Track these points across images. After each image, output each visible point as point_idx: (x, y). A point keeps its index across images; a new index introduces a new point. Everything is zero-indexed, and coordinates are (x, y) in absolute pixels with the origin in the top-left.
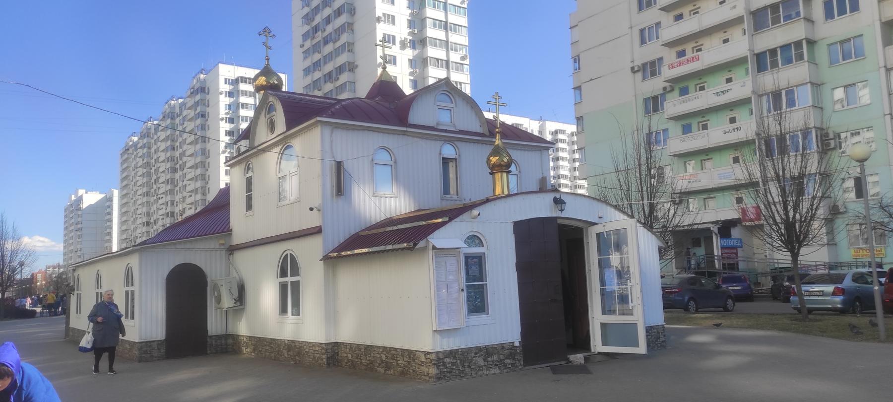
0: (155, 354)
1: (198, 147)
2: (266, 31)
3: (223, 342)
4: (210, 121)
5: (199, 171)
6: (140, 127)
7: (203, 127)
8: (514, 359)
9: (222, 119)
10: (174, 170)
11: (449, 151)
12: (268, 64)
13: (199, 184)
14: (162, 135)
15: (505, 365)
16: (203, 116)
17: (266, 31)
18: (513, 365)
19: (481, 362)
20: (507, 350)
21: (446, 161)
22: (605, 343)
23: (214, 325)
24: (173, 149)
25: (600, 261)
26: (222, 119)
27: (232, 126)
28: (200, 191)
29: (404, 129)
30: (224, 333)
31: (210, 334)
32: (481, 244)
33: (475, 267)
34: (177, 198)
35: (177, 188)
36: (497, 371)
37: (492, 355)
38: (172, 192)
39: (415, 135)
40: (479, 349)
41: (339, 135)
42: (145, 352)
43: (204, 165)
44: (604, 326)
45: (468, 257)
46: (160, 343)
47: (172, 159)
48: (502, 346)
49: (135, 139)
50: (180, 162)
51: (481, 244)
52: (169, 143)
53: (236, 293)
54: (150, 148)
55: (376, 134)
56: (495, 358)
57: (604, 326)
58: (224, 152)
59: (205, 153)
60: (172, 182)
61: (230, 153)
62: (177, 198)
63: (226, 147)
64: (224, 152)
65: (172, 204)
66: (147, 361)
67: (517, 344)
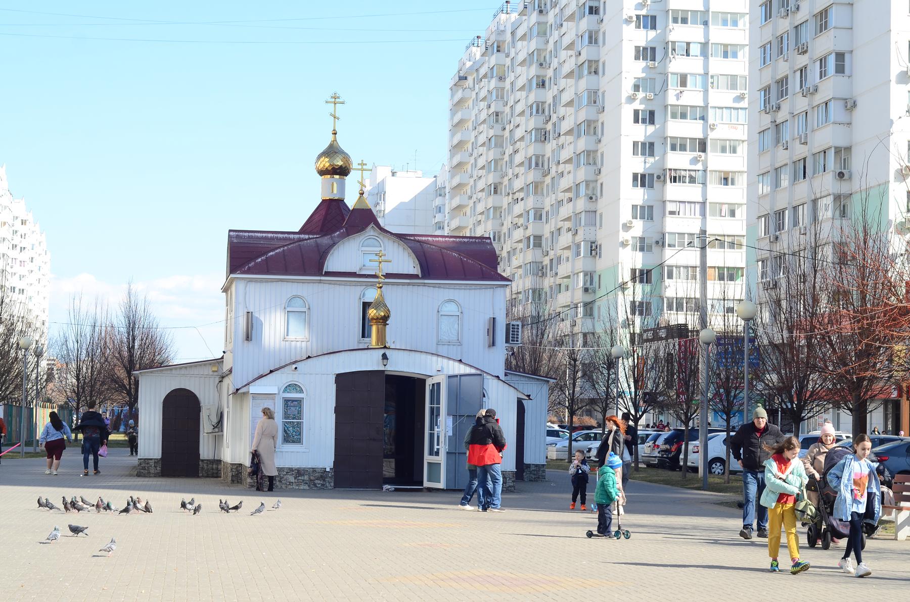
0: (152, 471)
1: (583, 84)
2: (335, 99)
3: (214, 466)
4: (607, 26)
5: (582, 144)
6: (483, 25)
7: (593, 38)
8: (324, 480)
9: (628, 21)
10: (543, 136)
11: (371, 295)
12: (335, 140)
13: (582, 174)
14: (523, 49)
15: (315, 485)
16: (593, 11)
17: (335, 99)
18: (323, 485)
19: (292, 479)
20: (322, 474)
21: (366, 306)
22: (429, 480)
23: (205, 452)
24: (542, 84)
25: (432, 410)
26: (628, 21)
27: (652, 34)
28: (583, 188)
29: (318, 278)
30: (211, 457)
31: (201, 458)
32: (301, 391)
33: (293, 408)
34: (548, 202)
35: (548, 180)
36: (306, 487)
37: (303, 475)
38: (537, 187)
39: (330, 283)
40: (291, 470)
41: (252, 286)
42: (144, 468)
43: (591, 128)
44: (429, 463)
45: (287, 401)
46: (156, 461)
47: (539, 108)
48: (314, 470)
49: (477, 52)
50: (554, 118)
51: (301, 391)
52: (533, 70)
53: (215, 420)
54: (501, 79)
55: (290, 284)
56: (306, 478)
57: (429, 463)
58: (631, 99)
59: (594, 98)
60: (538, 162)
61: (646, 100)
62: (548, 202)
63: (636, 88)
64: (631, 99)
65: (538, 217)
66: (145, 476)
67: (328, 470)
